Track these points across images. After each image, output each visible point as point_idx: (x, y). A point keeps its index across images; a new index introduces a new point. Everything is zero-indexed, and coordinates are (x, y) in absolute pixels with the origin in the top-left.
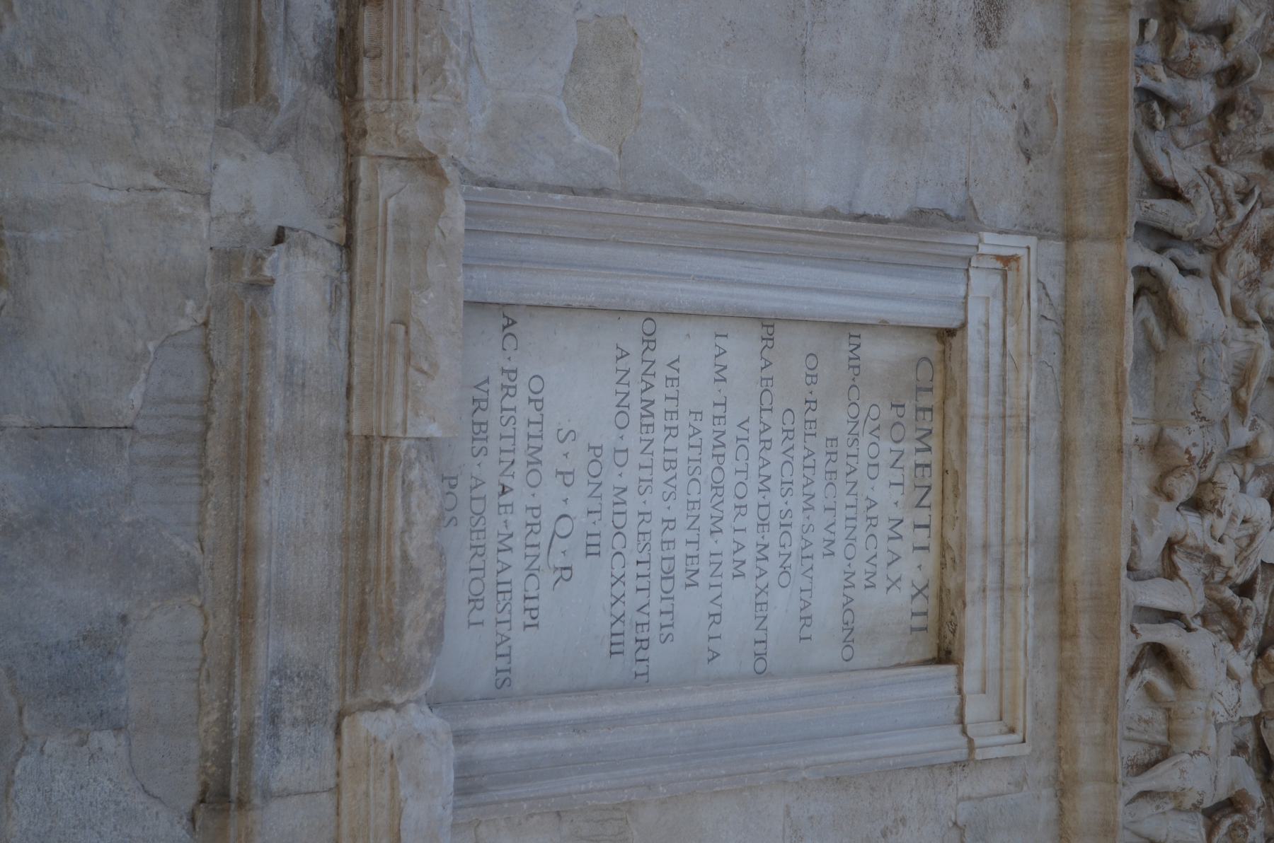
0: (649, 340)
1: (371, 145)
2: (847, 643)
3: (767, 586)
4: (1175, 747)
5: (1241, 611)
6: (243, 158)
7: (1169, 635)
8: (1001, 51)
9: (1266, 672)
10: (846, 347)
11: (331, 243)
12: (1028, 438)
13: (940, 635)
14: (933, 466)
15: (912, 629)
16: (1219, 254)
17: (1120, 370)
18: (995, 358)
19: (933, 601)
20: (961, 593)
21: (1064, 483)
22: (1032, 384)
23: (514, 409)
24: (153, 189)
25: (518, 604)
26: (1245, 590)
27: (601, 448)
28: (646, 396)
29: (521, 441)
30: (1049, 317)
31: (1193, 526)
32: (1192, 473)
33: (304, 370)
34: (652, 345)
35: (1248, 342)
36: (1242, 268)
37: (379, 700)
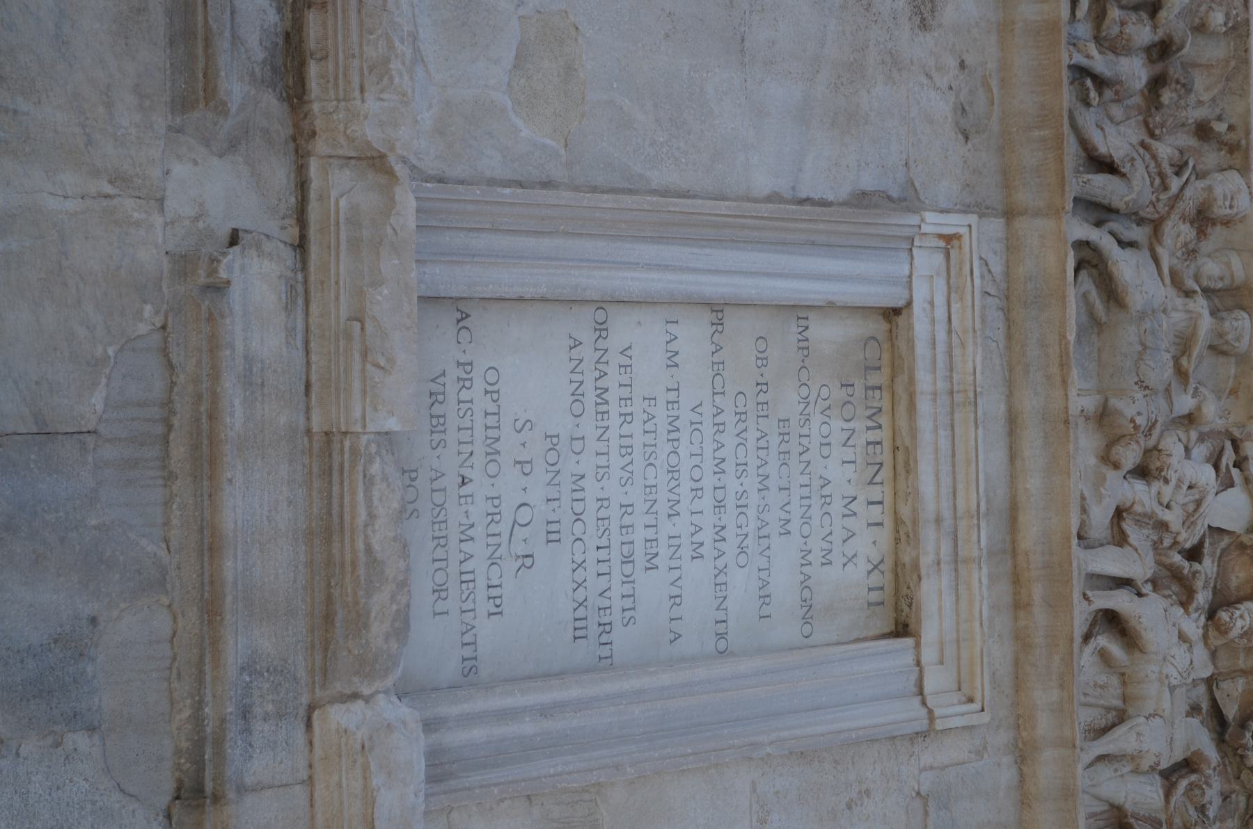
0: (601, 329)
1: (320, 146)
2: (806, 620)
3: (725, 567)
4: (1131, 711)
5: (1190, 575)
6: (196, 163)
7: (1120, 601)
9: (1216, 633)
10: (794, 329)
11: (285, 243)
12: (976, 413)
13: (897, 609)
15: (869, 604)
16: (1156, 226)
17: (1063, 342)
18: (941, 336)
19: (889, 576)
20: (916, 566)
21: (1013, 455)
22: (979, 359)
23: (471, 401)
24: (107, 196)
25: (481, 593)
26: (1194, 554)
27: (557, 436)
28: (600, 384)
29: (479, 432)
30: (992, 292)
31: (1140, 494)
32: (1137, 442)
33: (262, 370)
34: (604, 334)
35: (1188, 312)
36: (1179, 239)
37: (348, 691)
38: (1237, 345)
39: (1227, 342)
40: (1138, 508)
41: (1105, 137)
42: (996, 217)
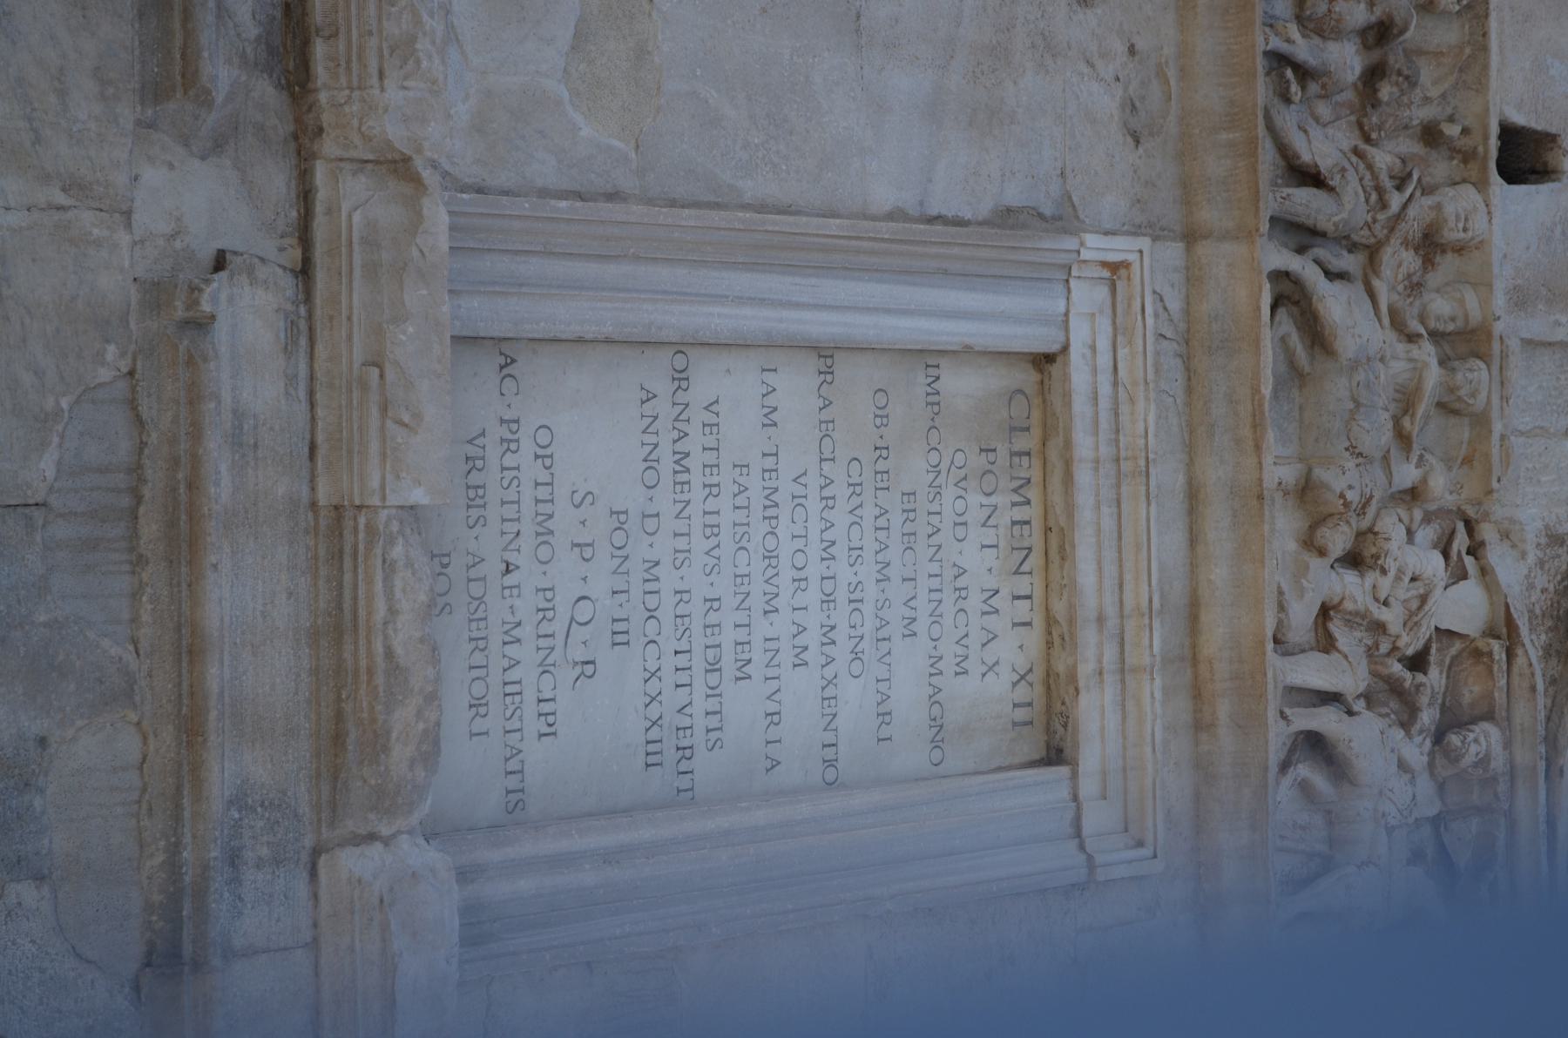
0: (681, 378)
1: (329, 146)
2: (936, 744)
3: (835, 677)
5: (1412, 689)
6: (171, 166)
7: (1326, 720)
8: (1099, 11)
11: (285, 268)
12: (1148, 485)
13: (1049, 730)
14: (1033, 522)
15: (1015, 724)
16: (1372, 253)
17: (1257, 398)
18: (1105, 389)
19: (1039, 689)
20: (1072, 677)
23: (518, 468)
24: (60, 208)
25: (530, 709)
26: (1417, 663)
27: (626, 512)
28: (679, 447)
30: (1169, 335)
31: (1352, 587)
32: (1348, 522)
33: (256, 427)
34: (684, 384)
35: (1411, 360)
36: (1401, 270)
37: (363, 831)
38: (1471, 401)
39: (1459, 399)
40: (1348, 606)
41: (1309, 141)
42: (1174, 240)
